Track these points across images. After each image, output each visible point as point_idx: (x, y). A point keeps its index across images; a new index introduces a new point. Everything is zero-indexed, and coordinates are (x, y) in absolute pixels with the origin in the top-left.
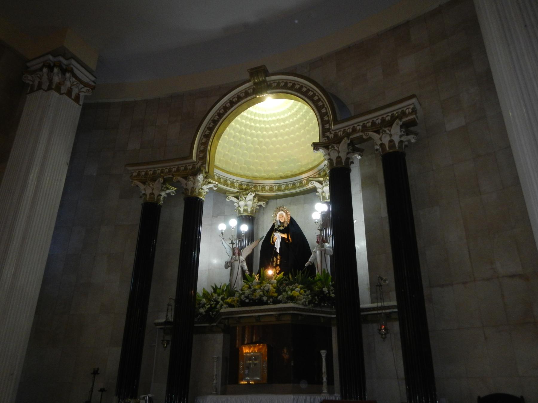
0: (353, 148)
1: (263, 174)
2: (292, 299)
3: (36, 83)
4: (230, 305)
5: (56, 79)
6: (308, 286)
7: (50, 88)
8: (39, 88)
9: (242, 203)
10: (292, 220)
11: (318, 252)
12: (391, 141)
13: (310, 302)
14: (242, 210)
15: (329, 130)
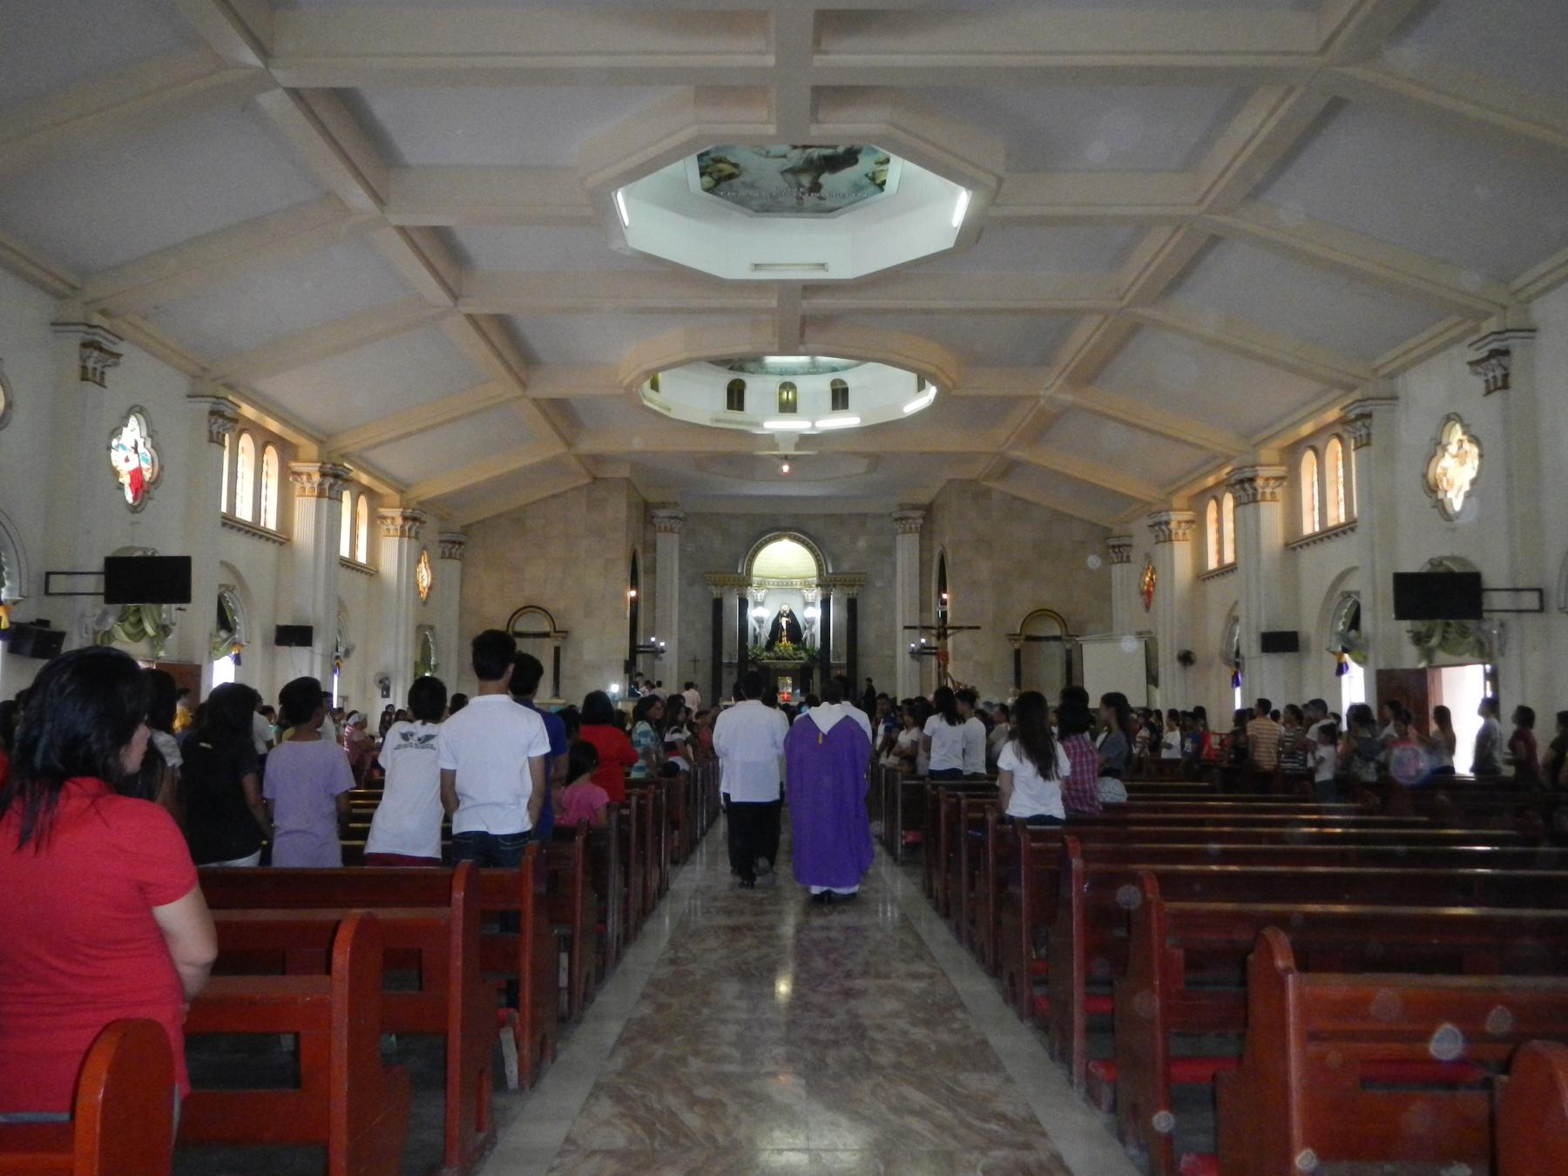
0: (835, 586)
1: (766, 574)
2: (801, 658)
3: (662, 525)
4: (769, 658)
5: (674, 525)
6: (806, 651)
7: (672, 531)
8: (666, 530)
9: (759, 595)
10: (791, 611)
11: (809, 634)
12: (853, 594)
13: (809, 659)
14: (759, 598)
15: (823, 575)
